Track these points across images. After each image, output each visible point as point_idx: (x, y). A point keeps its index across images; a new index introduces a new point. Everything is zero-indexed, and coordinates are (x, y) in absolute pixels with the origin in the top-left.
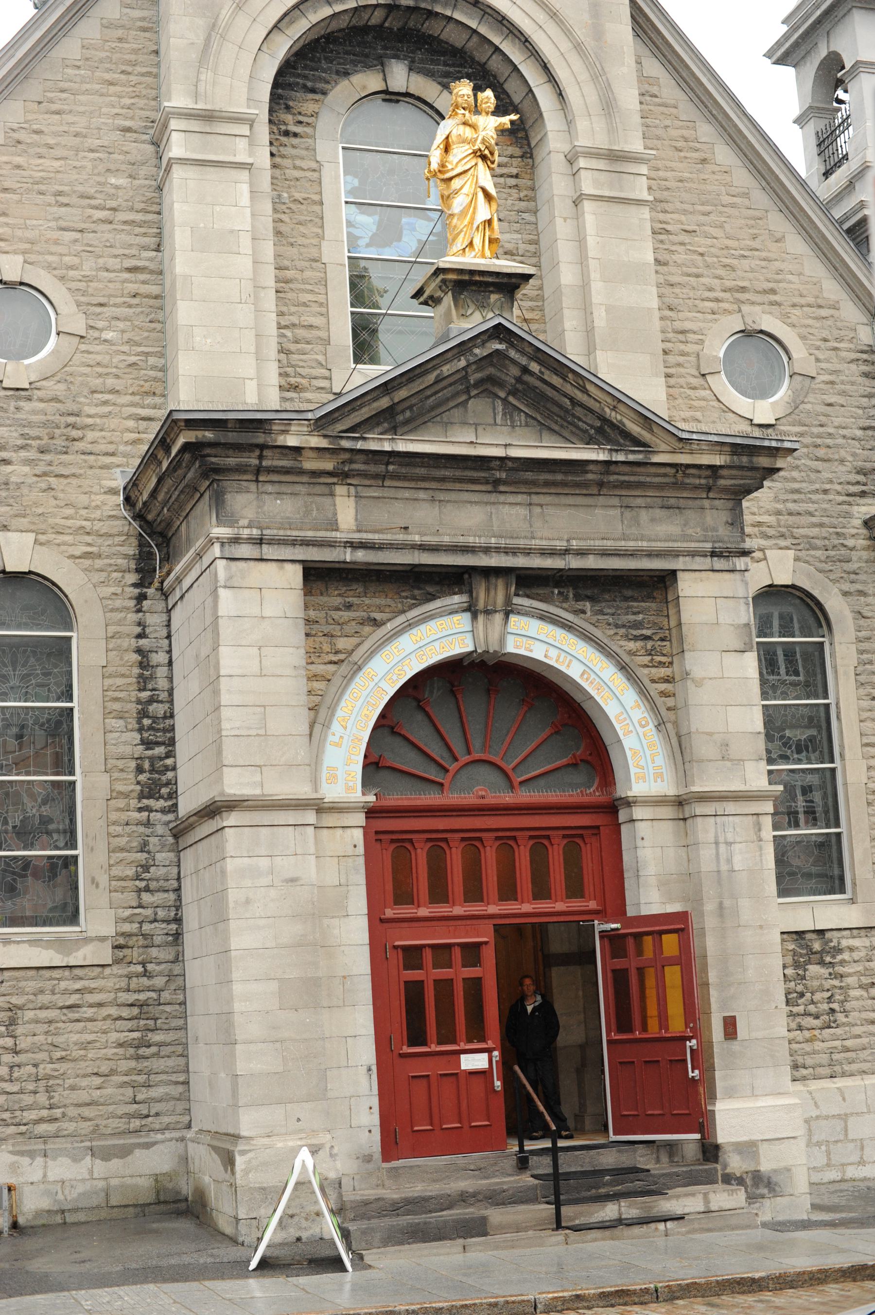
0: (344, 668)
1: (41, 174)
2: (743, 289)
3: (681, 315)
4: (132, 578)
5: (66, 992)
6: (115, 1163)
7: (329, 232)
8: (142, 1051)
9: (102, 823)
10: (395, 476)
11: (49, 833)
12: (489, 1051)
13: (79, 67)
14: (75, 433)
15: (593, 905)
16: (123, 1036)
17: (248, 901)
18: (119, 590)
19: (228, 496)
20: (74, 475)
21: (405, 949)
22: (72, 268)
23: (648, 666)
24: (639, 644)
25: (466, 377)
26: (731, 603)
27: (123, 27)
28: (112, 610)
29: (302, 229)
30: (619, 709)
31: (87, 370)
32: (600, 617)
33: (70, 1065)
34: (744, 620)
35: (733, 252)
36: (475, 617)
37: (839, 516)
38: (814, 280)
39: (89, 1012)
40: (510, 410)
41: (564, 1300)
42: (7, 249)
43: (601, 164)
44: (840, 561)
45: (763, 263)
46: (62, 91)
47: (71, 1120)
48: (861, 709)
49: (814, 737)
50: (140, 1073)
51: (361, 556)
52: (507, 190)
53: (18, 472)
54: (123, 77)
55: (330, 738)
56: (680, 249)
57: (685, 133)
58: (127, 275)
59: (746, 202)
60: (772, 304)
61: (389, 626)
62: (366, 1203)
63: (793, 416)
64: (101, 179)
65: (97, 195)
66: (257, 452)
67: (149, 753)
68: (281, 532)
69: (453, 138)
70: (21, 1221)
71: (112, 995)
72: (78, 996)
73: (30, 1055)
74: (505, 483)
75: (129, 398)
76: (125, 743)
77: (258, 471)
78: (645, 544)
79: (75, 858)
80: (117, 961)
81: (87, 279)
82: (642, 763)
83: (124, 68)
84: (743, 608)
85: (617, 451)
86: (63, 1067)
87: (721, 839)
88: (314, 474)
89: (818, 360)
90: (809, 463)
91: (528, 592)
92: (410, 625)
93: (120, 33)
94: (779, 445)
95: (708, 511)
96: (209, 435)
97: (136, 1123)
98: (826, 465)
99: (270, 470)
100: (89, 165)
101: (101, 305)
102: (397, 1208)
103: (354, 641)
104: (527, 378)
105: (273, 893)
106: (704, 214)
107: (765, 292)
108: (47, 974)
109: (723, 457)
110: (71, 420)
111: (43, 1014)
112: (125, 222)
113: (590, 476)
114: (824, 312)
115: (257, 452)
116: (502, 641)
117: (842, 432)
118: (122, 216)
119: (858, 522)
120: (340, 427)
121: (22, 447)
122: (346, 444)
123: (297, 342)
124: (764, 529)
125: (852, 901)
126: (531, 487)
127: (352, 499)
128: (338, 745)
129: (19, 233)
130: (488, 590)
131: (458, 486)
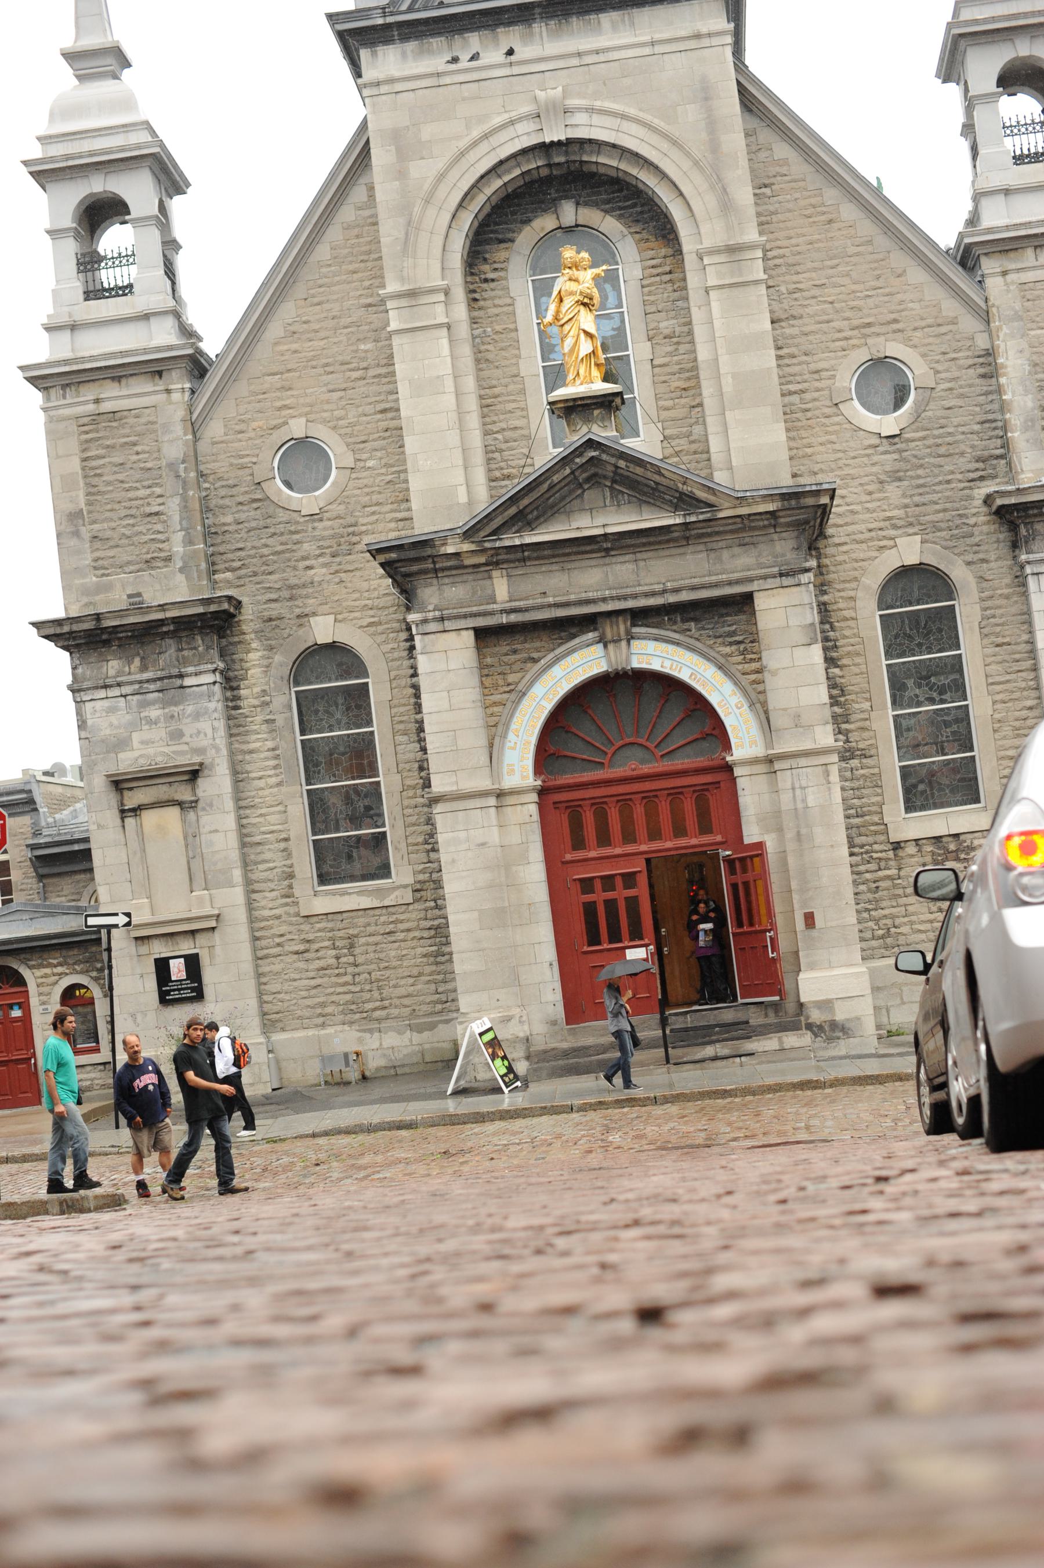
0: (513, 696)
1: (312, 353)
2: (869, 325)
3: (815, 358)
5: (384, 923)
6: (426, 1034)
7: (524, 353)
8: (439, 959)
9: (399, 808)
10: (529, 558)
11: (371, 817)
12: (646, 946)
13: (330, 265)
14: (355, 539)
15: (719, 838)
16: (424, 950)
17: (453, 861)
18: (396, 646)
19: (419, 591)
20: (356, 569)
21: (580, 880)
22: (340, 419)
23: (741, 663)
24: (734, 648)
25: (576, 478)
26: (799, 609)
27: (358, 226)
28: (392, 660)
29: (504, 353)
30: (720, 698)
31: (358, 492)
32: (702, 632)
33: (392, 971)
34: (809, 621)
35: (858, 294)
36: (605, 646)
37: (962, 500)
38: (934, 303)
39: (402, 936)
40: (615, 494)
41: (591, 1105)
42: (295, 414)
43: (722, 258)
44: (964, 537)
45: (886, 299)
46: (320, 287)
47: (396, 1007)
48: (985, 656)
49: (955, 680)
50: (439, 973)
51: (513, 618)
52: (663, 286)
53: (319, 573)
54: (362, 265)
55: (508, 745)
56: (812, 302)
57: (813, 201)
58: (379, 416)
59: (870, 249)
60: (894, 332)
61: (543, 662)
62: (545, 1052)
63: (916, 424)
64: (354, 348)
65: (353, 360)
66: (430, 560)
68: (455, 611)
69: (563, 293)
70: (367, 1074)
71: (416, 923)
72: (392, 926)
73: (365, 967)
74: (612, 549)
75: (390, 507)
76: (410, 752)
77: (436, 571)
78: (724, 576)
79: (384, 833)
80: (415, 901)
81: (351, 425)
82: (741, 735)
83: (362, 258)
84: (808, 611)
85: (689, 514)
86: (388, 973)
87: (797, 785)
88: (475, 566)
89: (937, 372)
90: (932, 460)
91: (645, 622)
92: (557, 660)
93: (356, 231)
94: (819, 488)
95: (777, 543)
96: (393, 555)
97: (439, 1007)
98: (947, 460)
99: (443, 569)
100: (343, 338)
101: (364, 442)
102: (566, 1054)
103: (519, 675)
104: (620, 471)
105: (470, 854)
106: (832, 268)
107: (889, 323)
108: (371, 912)
109: (775, 504)
110: (351, 529)
111: (371, 939)
112: (374, 377)
113: (676, 534)
114: (943, 329)
115: (430, 560)
116: (628, 660)
117: (961, 429)
118: (371, 372)
119: (979, 502)
120: (482, 534)
121: (320, 555)
122: (487, 545)
123: (506, 442)
124: (893, 522)
126: (633, 549)
127: (505, 578)
128: (513, 748)
129: (302, 401)
130: (611, 626)
131: (580, 557)
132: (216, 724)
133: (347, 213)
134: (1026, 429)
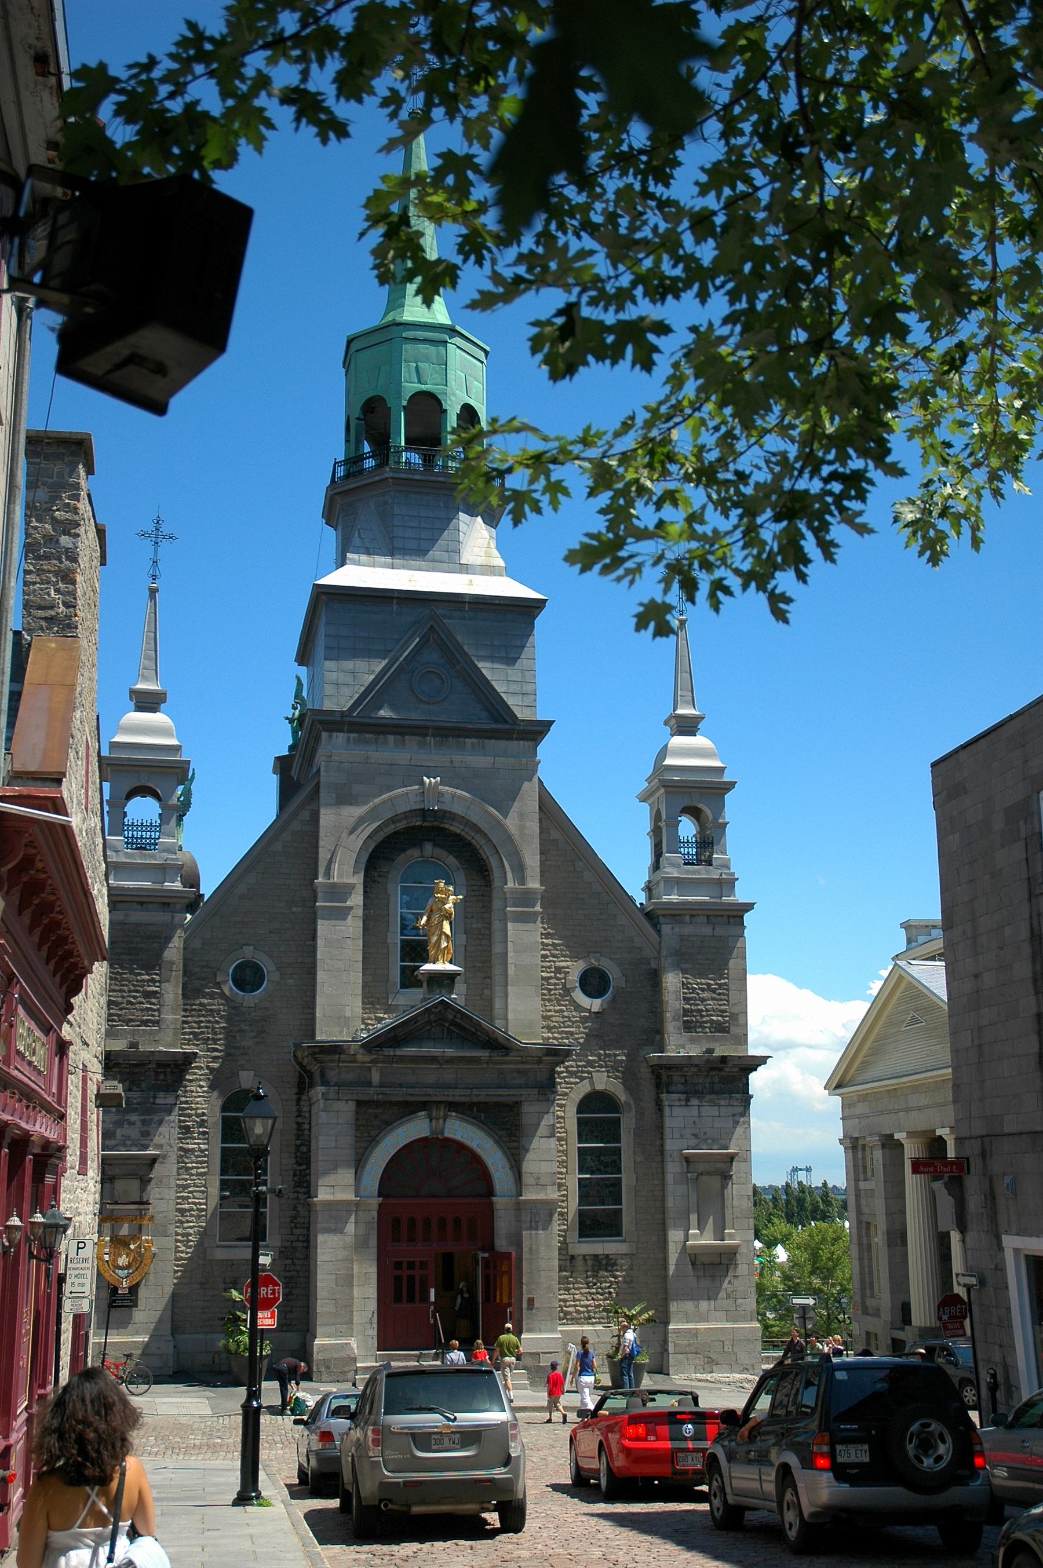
4: (295, 1090)
7: (391, 929)
36: (431, 1120)
67: (299, 1168)
125: (625, 1241)
132: (172, 1131)
133: (296, 826)
134: (674, 1019)
